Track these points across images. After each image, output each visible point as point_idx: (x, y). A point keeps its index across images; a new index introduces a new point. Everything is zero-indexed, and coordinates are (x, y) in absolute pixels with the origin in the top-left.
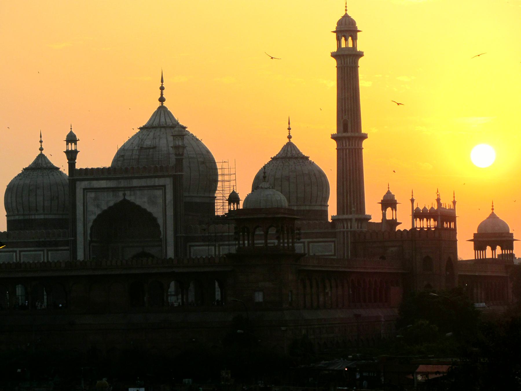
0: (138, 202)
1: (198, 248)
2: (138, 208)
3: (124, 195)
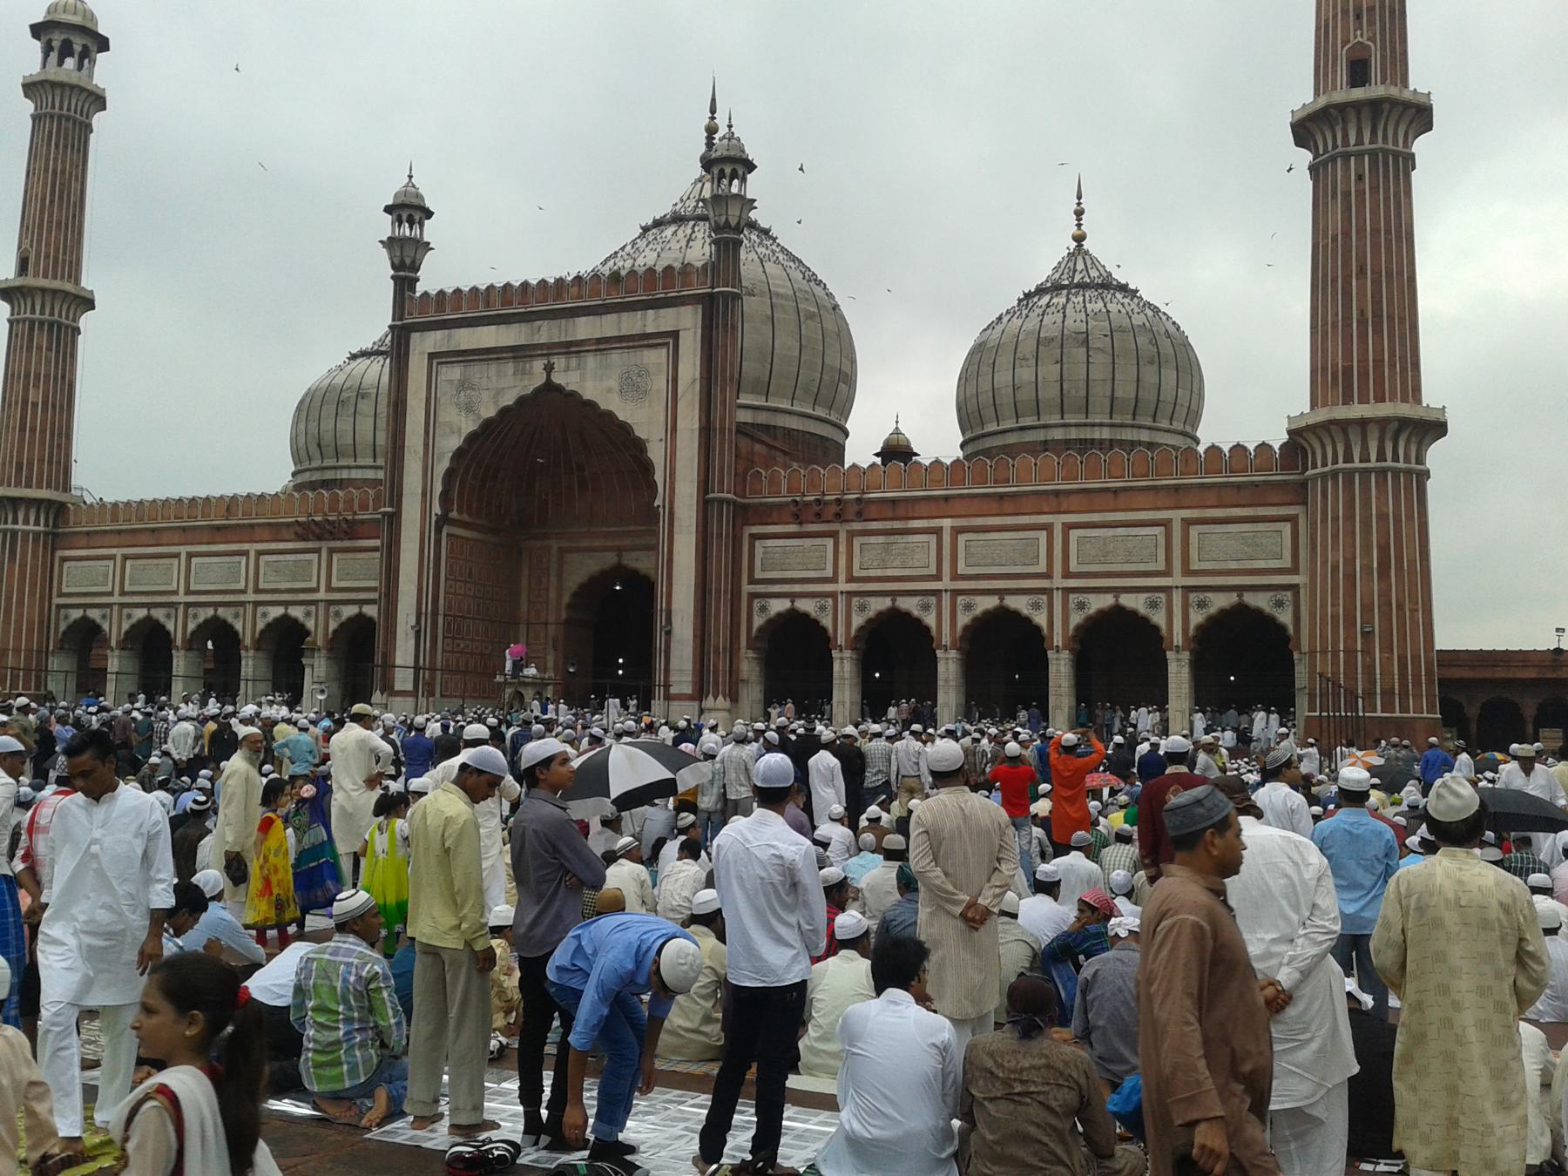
0: (590, 391)
2: (591, 405)
3: (549, 369)
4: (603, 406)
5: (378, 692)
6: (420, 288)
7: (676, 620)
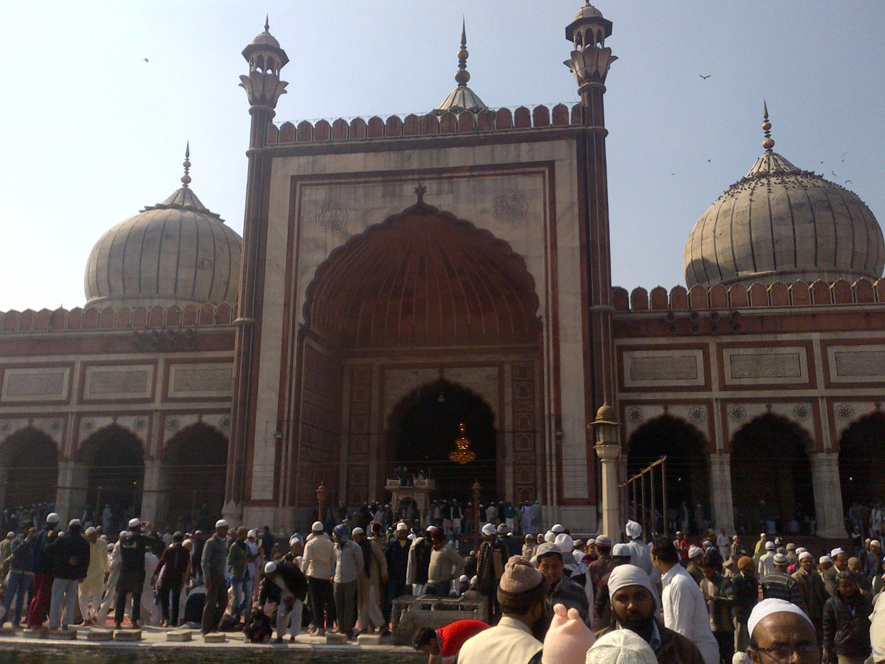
0: (464, 211)
1: (644, 354)
2: (465, 225)
3: (421, 192)
4: (477, 227)
5: (232, 500)
6: (278, 121)
7: (567, 425)
